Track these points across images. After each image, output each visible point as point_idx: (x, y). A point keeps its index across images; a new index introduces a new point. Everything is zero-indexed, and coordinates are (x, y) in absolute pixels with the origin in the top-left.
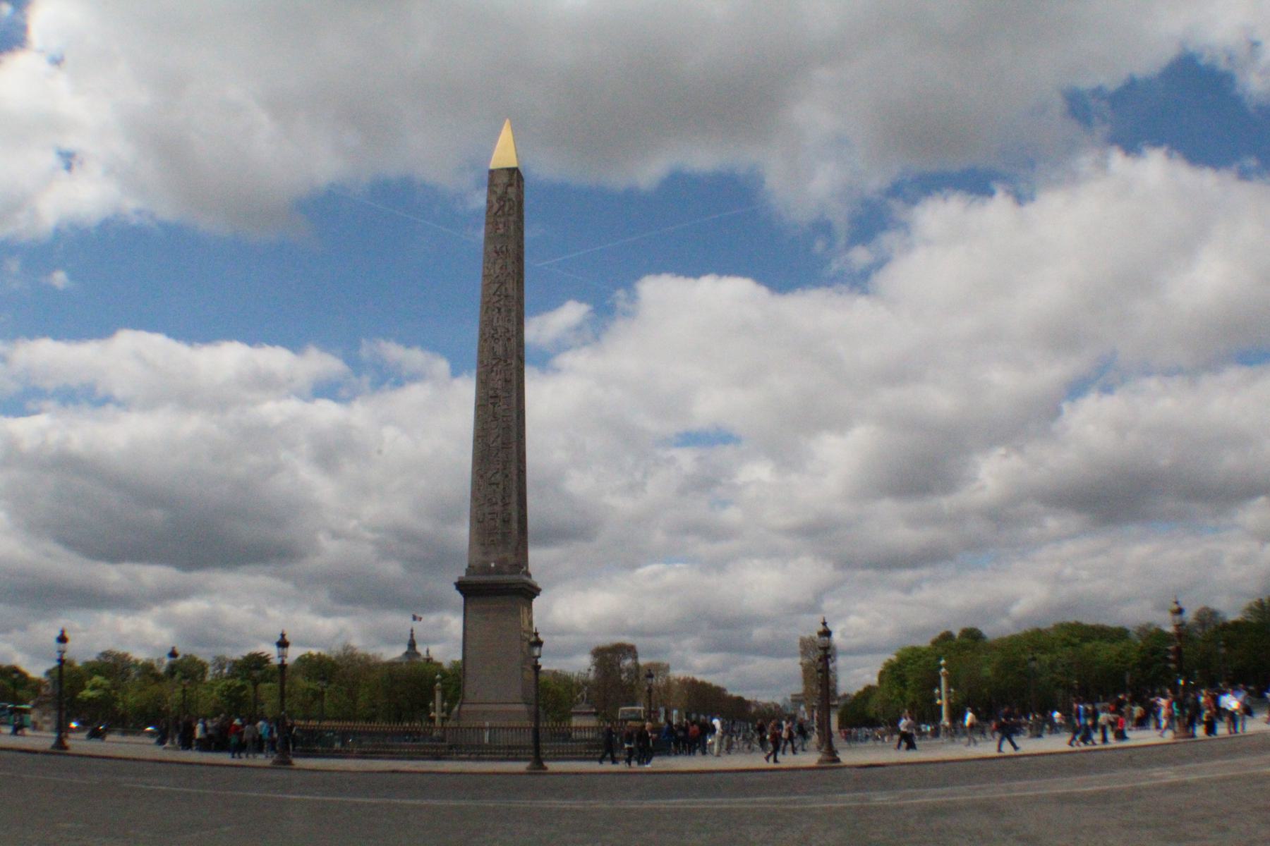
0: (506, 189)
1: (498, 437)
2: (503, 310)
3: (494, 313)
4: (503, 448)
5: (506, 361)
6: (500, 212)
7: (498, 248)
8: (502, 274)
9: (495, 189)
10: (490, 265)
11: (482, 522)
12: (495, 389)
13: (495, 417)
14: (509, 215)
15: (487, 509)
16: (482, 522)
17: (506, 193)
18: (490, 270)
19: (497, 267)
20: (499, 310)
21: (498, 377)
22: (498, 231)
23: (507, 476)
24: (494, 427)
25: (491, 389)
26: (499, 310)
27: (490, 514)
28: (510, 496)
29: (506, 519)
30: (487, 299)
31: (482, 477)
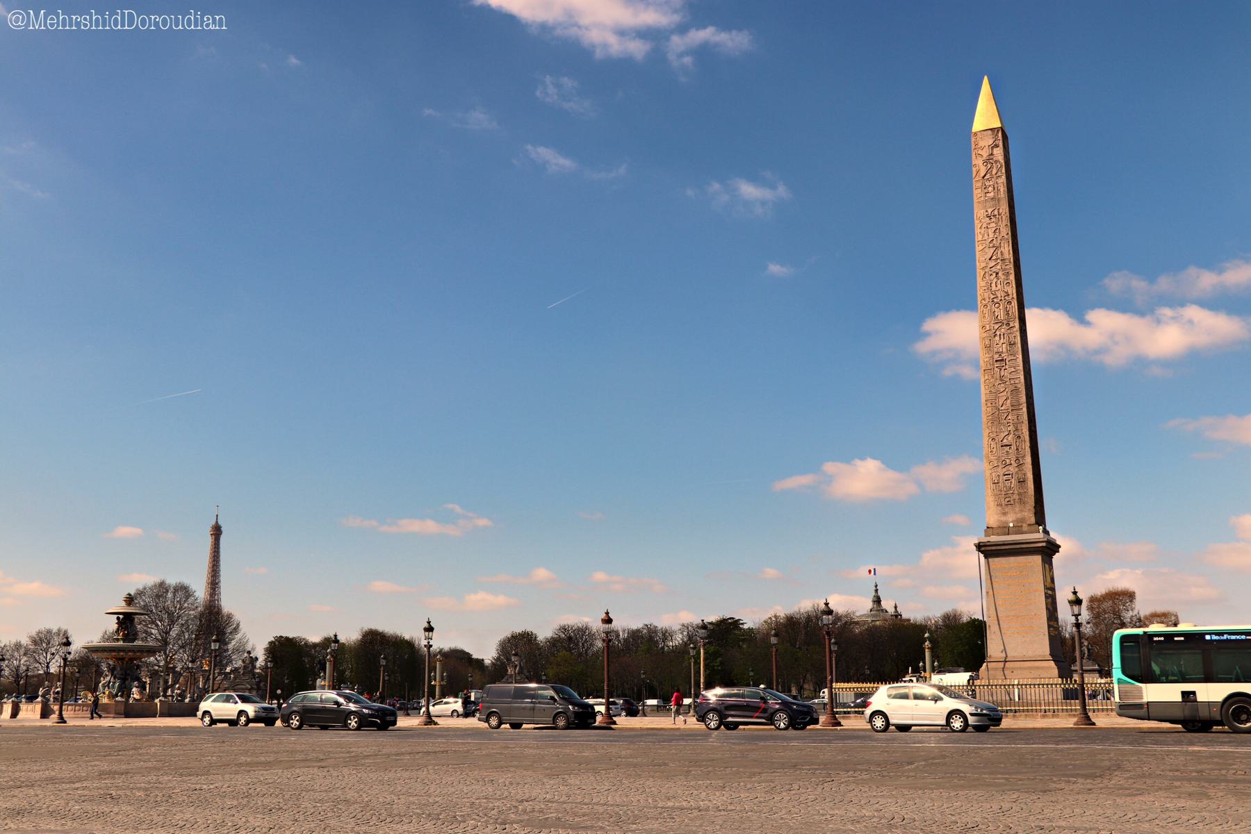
0: (992, 149)
2: (1000, 274)
3: (992, 277)
4: (1012, 410)
5: (1008, 324)
7: (990, 212)
10: (983, 230)
11: (998, 483)
12: (1000, 353)
13: (1001, 380)
15: (1001, 471)
16: (998, 483)
17: (992, 154)
19: (991, 231)
21: (1002, 341)
22: (988, 195)
23: (1019, 437)
24: (1002, 390)
26: (997, 274)
28: (1024, 457)
29: (1021, 480)
30: (983, 265)
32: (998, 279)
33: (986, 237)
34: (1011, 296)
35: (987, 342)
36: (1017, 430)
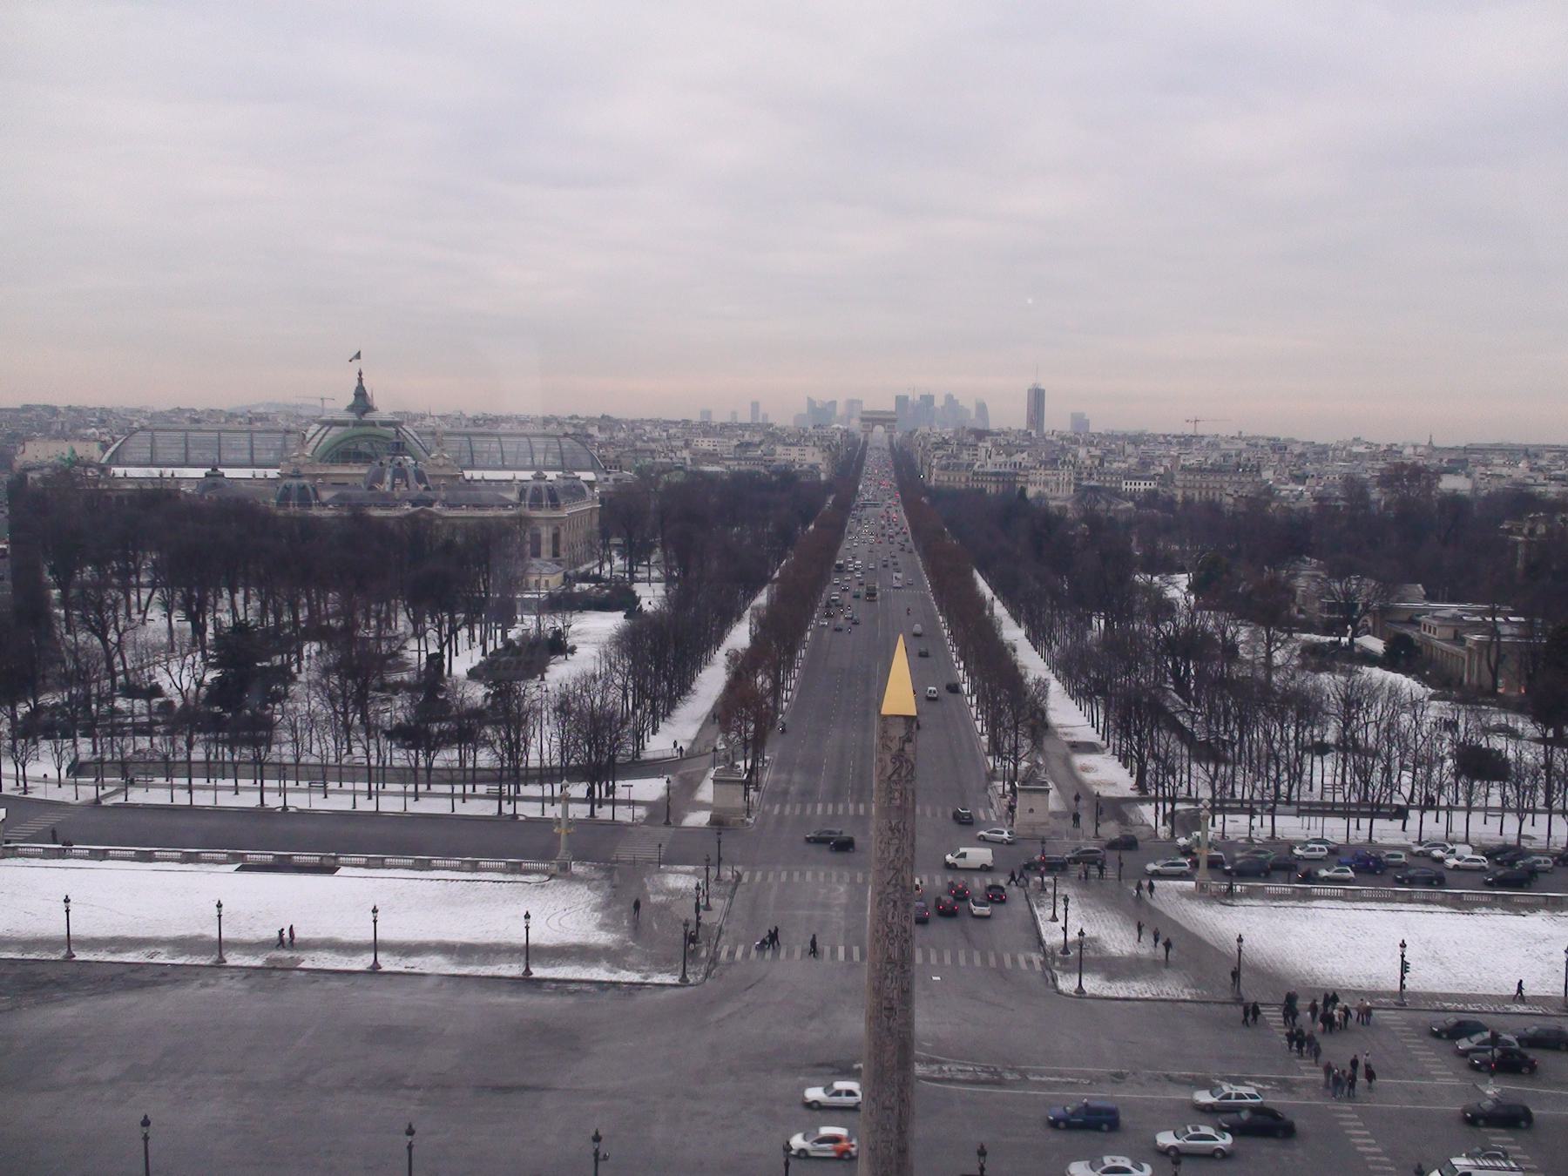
0: (904, 744)
1: (893, 1055)
2: (899, 903)
3: (889, 906)
5: (902, 967)
6: (895, 777)
8: (899, 859)
9: (889, 743)
10: (883, 845)
11: (876, 1149)
12: (890, 1000)
14: (907, 781)
17: (903, 750)
18: (883, 853)
20: (895, 902)
22: (893, 802)
23: (903, 1101)
25: (886, 998)
26: (895, 902)
27: (883, 1141)
31: (874, 1099)
32: (895, 909)
33: (886, 855)
34: (908, 933)
35: (877, 984)
36: (902, 1091)
